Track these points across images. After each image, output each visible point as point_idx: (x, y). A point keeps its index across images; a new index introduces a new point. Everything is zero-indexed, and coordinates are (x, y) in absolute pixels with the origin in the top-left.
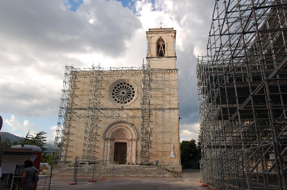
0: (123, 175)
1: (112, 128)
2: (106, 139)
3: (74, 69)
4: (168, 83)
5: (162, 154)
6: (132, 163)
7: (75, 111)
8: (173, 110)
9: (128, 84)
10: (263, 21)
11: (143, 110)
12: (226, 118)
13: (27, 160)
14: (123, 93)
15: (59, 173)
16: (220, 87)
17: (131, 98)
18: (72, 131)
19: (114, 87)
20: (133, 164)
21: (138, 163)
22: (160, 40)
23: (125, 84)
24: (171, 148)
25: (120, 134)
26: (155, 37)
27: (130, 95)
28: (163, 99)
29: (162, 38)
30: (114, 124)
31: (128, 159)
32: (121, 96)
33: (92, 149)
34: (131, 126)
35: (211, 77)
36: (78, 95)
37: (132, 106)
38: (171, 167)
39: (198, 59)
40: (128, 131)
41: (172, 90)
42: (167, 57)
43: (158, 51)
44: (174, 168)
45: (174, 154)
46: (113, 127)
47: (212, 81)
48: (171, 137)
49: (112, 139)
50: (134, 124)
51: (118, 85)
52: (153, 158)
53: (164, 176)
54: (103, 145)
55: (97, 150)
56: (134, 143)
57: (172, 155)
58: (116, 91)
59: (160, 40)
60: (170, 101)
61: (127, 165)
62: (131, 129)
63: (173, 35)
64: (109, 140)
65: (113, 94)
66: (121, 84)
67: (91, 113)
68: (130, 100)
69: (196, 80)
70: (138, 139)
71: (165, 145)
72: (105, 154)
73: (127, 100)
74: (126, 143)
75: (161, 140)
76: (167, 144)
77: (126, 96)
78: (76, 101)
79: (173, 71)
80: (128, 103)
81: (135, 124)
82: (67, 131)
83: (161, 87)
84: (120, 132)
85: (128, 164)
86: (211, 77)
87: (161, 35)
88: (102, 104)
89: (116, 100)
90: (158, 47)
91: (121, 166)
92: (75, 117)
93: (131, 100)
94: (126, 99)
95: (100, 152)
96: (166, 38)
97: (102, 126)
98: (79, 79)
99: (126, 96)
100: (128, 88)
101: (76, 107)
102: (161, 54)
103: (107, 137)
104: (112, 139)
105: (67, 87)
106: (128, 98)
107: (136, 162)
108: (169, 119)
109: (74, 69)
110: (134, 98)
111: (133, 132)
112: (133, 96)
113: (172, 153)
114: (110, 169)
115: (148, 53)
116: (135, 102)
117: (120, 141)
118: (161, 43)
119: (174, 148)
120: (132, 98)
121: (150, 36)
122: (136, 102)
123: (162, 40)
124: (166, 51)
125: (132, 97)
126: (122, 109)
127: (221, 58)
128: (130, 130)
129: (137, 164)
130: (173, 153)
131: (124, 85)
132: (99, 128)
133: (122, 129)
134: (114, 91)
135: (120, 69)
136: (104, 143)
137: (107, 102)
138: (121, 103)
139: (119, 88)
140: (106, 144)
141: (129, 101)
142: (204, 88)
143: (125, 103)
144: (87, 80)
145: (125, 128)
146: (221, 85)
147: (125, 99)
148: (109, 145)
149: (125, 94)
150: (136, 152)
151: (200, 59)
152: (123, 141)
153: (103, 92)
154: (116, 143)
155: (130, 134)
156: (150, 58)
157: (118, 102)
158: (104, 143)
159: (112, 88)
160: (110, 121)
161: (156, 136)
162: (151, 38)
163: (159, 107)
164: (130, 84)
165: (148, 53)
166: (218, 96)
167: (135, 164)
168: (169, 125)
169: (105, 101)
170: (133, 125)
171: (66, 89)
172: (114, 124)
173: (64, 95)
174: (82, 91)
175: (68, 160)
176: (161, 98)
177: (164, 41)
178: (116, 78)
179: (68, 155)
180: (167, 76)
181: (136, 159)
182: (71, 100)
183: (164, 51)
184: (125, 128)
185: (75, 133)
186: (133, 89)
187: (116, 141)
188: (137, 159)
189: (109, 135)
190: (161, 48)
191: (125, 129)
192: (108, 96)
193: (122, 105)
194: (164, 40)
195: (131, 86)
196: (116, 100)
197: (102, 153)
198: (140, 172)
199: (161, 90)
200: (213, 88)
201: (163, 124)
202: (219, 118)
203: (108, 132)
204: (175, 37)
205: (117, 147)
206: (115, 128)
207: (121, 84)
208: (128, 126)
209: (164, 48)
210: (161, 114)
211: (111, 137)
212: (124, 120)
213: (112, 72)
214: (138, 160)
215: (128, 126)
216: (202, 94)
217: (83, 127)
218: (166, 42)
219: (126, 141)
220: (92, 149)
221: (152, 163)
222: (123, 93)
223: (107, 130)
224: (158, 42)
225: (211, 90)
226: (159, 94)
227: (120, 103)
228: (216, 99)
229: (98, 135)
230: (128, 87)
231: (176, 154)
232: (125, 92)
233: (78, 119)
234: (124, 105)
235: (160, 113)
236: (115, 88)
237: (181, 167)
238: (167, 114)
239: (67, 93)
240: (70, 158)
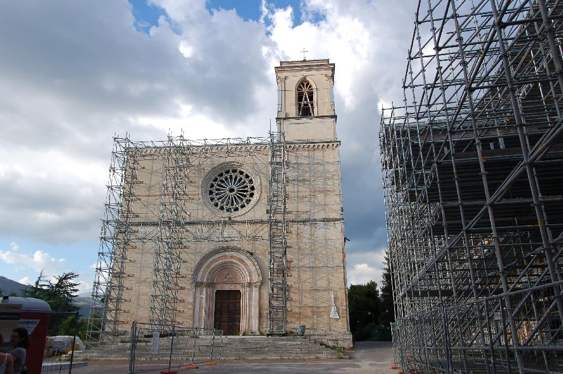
0: (234, 358)
1: (209, 261)
2: (198, 285)
3: (132, 143)
4: (321, 168)
5: (313, 312)
6: (252, 333)
7: (134, 228)
8: (332, 223)
9: (241, 173)
10: (517, 30)
11: (272, 223)
12: (454, 229)
13: (24, 329)
14: (232, 190)
15: (102, 357)
16: (437, 163)
17: (248, 200)
18: (128, 269)
19: (213, 178)
20: (253, 334)
21: (263, 330)
22: (304, 83)
23: (234, 171)
24: (329, 300)
25: (225, 273)
26: (294, 79)
27: (245, 193)
28: (313, 200)
29: (308, 79)
31: (243, 325)
32: (227, 196)
33: (169, 303)
34: (247, 257)
35: (415, 147)
36: (140, 196)
37: (249, 217)
38: (330, 337)
39: (383, 112)
40: (243, 267)
41: (329, 182)
42: (317, 117)
43: (300, 105)
44: (337, 340)
45: (338, 311)
46: (211, 259)
47: (416, 154)
48: (330, 277)
49: (210, 285)
50: (253, 251)
51: (221, 175)
52: (293, 320)
53: (317, 358)
55: (180, 307)
56: (255, 293)
57: (333, 314)
58: (218, 187)
59: (304, 83)
60: (325, 205)
61: (241, 336)
62: (249, 262)
63: (330, 73)
64: (203, 286)
65: (211, 193)
66: (227, 172)
67: (166, 232)
68: (246, 204)
69: (377, 156)
70: (262, 283)
71: (318, 294)
72: (197, 317)
73: (240, 205)
74: (239, 291)
75: (310, 283)
76: (321, 292)
77: (237, 196)
78: (135, 207)
79: (331, 144)
80: (241, 211)
81: (257, 252)
82: (118, 270)
83: (307, 176)
84: (226, 268)
85: (244, 335)
86: (415, 147)
87: (305, 73)
88: (188, 213)
89: (216, 205)
90: (300, 97)
91: (230, 339)
92: (134, 241)
93: (248, 204)
94: (237, 203)
95: (186, 310)
96: (316, 78)
97: (190, 259)
98: (142, 163)
99: (237, 196)
100: (241, 179)
101: (137, 220)
102: (305, 111)
103: (199, 280)
104: (210, 285)
105: (117, 180)
106: (242, 200)
107: (259, 330)
108: (324, 241)
109: (132, 143)
110: (254, 200)
111: (253, 268)
112: (252, 195)
113: (333, 309)
114: (207, 346)
115: (279, 110)
116: (256, 207)
117: (227, 287)
118: (305, 90)
119: (336, 299)
120: (250, 200)
121: (283, 75)
122: (256, 208)
123: (308, 84)
124: (315, 105)
125: (248, 197)
126: (231, 222)
127: (441, 98)
128: (246, 265)
129: (261, 334)
130: (336, 310)
131: (232, 174)
132: (184, 262)
133: (232, 262)
134: (212, 186)
135: (225, 142)
136: (195, 293)
137: (198, 208)
138: (228, 210)
139: (222, 181)
140: (198, 295)
141: (243, 206)
142: (396, 172)
143: (236, 209)
144: (158, 165)
145: (237, 262)
146: (440, 158)
147: (235, 203)
148: (204, 296)
149: (234, 193)
150: (260, 309)
151: (387, 114)
152: (233, 288)
153: (190, 190)
154: (218, 291)
155: (247, 273)
156: (285, 119)
157: (222, 208)
159: (210, 178)
160: (206, 247)
161: (299, 276)
162: (285, 79)
163: (305, 216)
164: (246, 172)
165: (279, 110)
166: (434, 184)
167: (258, 333)
168: (324, 252)
169: (195, 206)
170: (252, 254)
171: (114, 184)
173: (112, 196)
174: (149, 188)
175: (120, 328)
176: (307, 199)
177: (311, 86)
178: (217, 161)
179: (121, 319)
180: (318, 154)
181: (259, 324)
182: (127, 207)
183: (312, 105)
184: (237, 262)
185: (135, 274)
186: (251, 181)
187: (219, 288)
189: (203, 277)
190: (306, 99)
192: (200, 196)
193: (226, 214)
194: (311, 83)
195: (247, 176)
196: (216, 205)
197: (191, 312)
198: (269, 350)
199: (307, 183)
200: (419, 167)
201: (312, 250)
202: (437, 230)
203: (202, 270)
204: (333, 77)
205: (220, 301)
206: (216, 261)
207: (227, 172)
208: (243, 257)
209: (311, 98)
210: (309, 231)
211: (208, 279)
212: (235, 244)
213: (207, 150)
214: (265, 325)
215: (243, 257)
216: (393, 184)
217: (150, 259)
218: (314, 87)
219: (238, 288)
220: (169, 303)
221: (293, 330)
222: (232, 190)
224: (300, 87)
225: (414, 172)
226: (304, 190)
227: (225, 210)
228: (428, 189)
229: (183, 277)
230: (241, 179)
231: (341, 311)
232: (236, 189)
233: (139, 244)
234: (234, 215)
235: (306, 229)
236: (216, 180)
237: (351, 337)
238: (320, 231)
239: (117, 193)
240: (124, 326)
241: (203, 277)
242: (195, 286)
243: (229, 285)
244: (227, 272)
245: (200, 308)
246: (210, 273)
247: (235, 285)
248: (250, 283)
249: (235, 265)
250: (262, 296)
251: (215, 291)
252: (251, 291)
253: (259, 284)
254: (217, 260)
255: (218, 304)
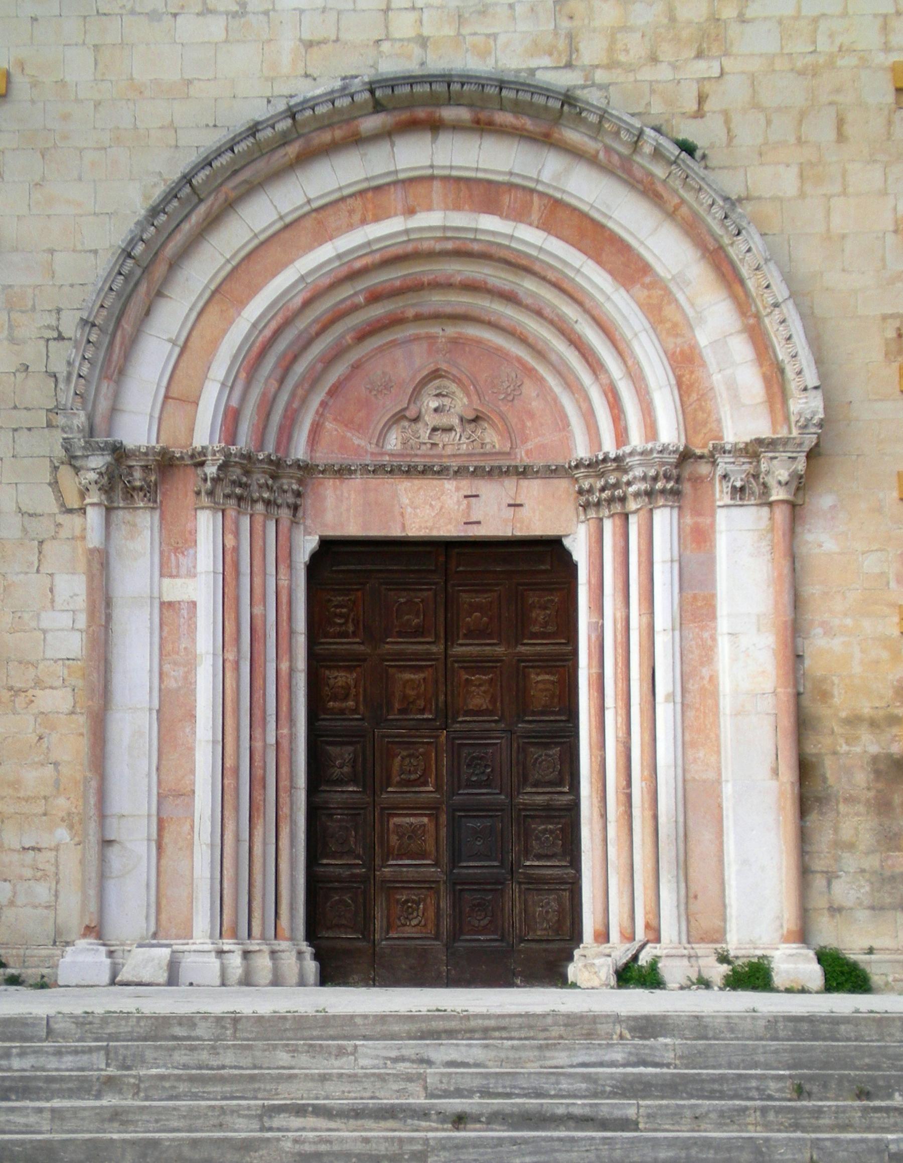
2: (136, 479)
25: (407, 361)
30: (284, 140)
31: (615, 879)
40: (594, 277)
46: (261, 214)
54: (73, 588)
56: (741, 541)
64: (185, 486)
104: (257, 481)
111: (713, 321)
117: (428, 512)
128: (630, 267)
145: (529, 237)
148: (199, 586)
150: (802, 723)
154: (331, 551)
158: (101, 567)
172: (284, 140)
187: (345, 511)
188: (818, 864)
189: (181, 386)
191: (520, 265)
197: (70, 747)
203: (172, 316)
206: (312, 234)
208: (586, 188)
215: (586, 188)
219: (535, 511)
223: (142, 272)
241: (177, 396)
242: (108, 490)
243: (450, 492)
244: (420, 360)
245: (172, 713)
246: (253, 359)
247: (510, 483)
248: (686, 456)
249: (529, 286)
250: (812, 590)
251: (306, 545)
252: (698, 539)
253: (779, 471)
254: (318, 220)
255: (340, 678)
